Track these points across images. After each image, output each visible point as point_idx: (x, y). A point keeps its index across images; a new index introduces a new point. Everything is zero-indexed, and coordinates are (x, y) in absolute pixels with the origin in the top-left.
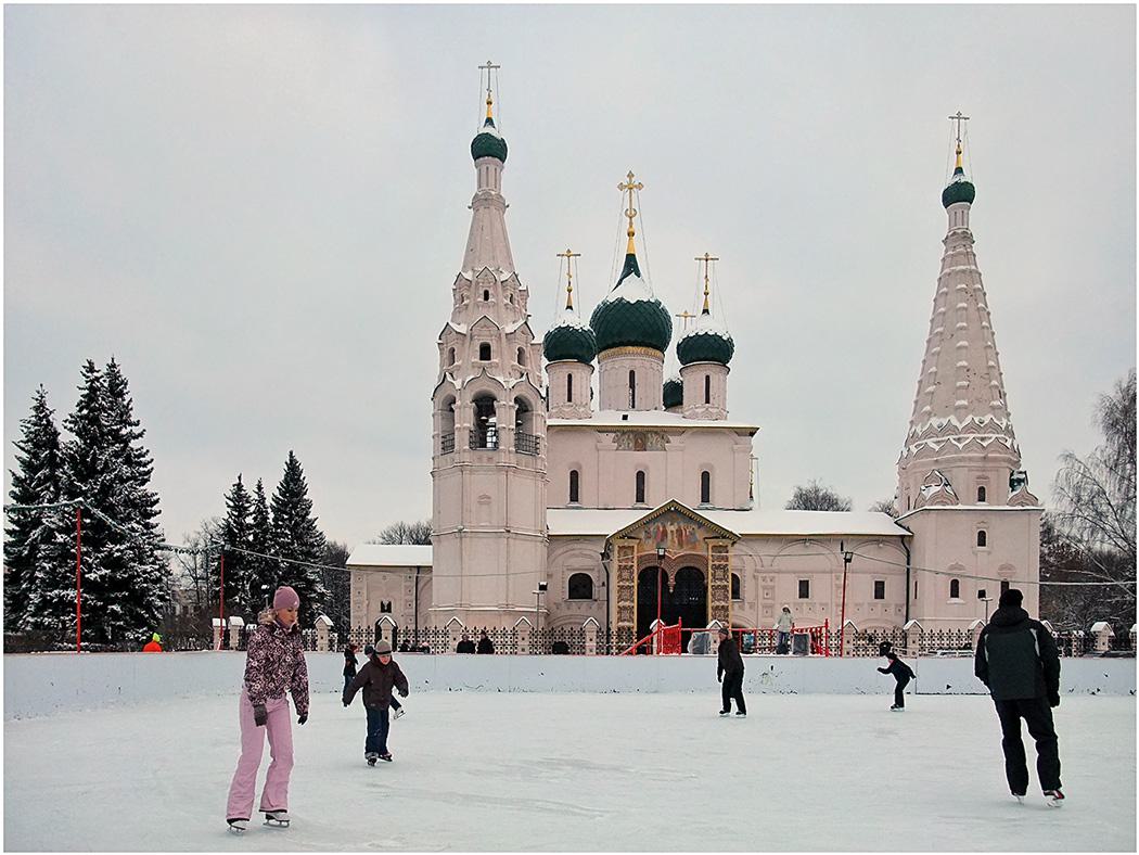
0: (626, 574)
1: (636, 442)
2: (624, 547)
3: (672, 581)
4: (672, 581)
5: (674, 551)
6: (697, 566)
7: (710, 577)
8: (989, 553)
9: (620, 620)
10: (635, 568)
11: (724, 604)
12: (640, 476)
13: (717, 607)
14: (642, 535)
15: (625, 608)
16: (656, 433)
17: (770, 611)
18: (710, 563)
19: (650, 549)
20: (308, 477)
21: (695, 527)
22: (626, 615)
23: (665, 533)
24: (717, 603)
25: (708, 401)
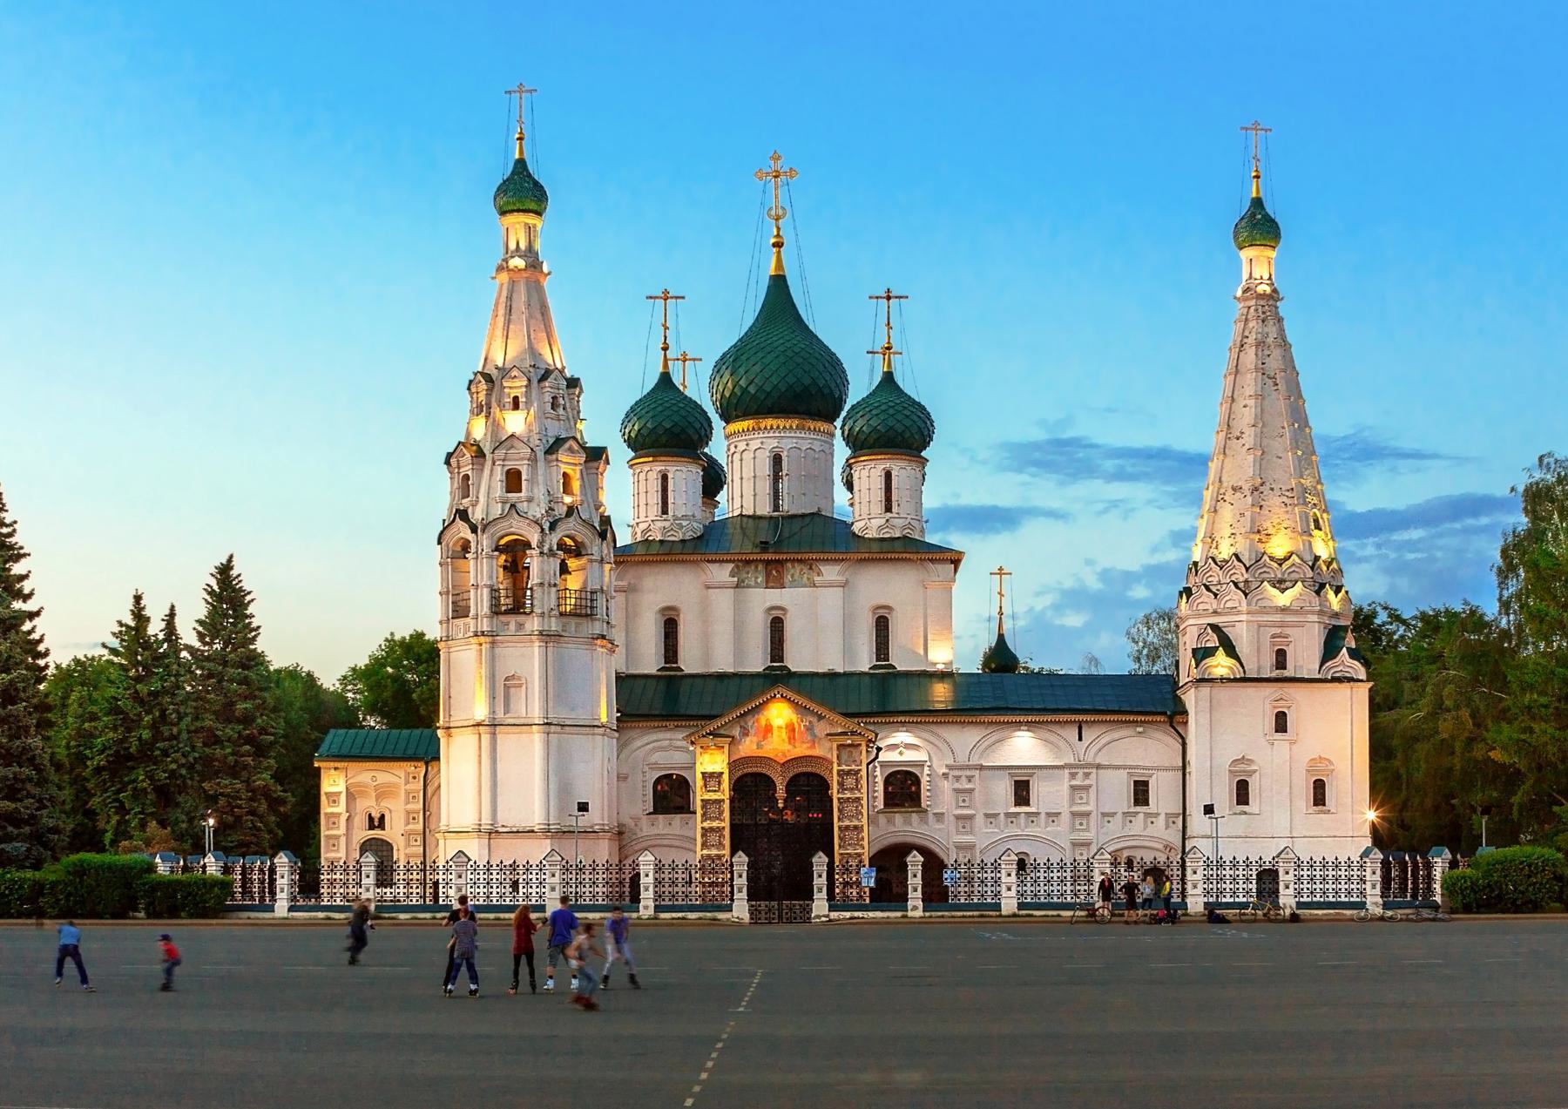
1: (768, 575)
3: (781, 792)
4: (781, 792)
7: (835, 791)
8: (1293, 742)
9: (704, 845)
10: (726, 777)
11: (856, 823)
12: (777, 627)
13: (847, 828)
14: (736, 732)
15: (712, 829)
16: (800, 561)
17: (968, 826)
18: (836, 768)
21: (814, 720)
22: (713, 838)
24: (847, 823)
25: (888, 509)
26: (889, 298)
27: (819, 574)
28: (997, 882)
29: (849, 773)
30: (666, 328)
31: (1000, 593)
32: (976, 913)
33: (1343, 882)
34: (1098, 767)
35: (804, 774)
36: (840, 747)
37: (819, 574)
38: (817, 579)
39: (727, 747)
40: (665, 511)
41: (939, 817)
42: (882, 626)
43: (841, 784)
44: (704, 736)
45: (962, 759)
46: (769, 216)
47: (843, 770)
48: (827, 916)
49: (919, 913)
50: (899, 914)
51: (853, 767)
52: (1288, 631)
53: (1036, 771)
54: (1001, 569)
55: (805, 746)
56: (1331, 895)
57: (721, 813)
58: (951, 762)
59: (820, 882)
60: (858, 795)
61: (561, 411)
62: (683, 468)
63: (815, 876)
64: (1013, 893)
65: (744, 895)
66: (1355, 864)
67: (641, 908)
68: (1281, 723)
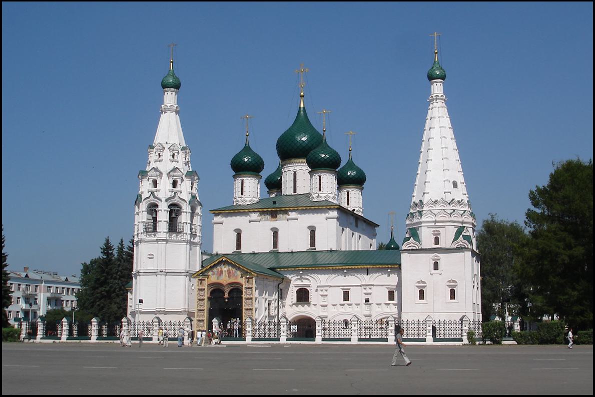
0: (202, 293)
3: (226, 295)
4: (226, 295)
5: (225, 279)
13: (247, 309)
18: (244, 286)
19: (213, 278)
23: (221, 272)
24: (247, 307)
25: (320, 190)
27: (289, 215)
29: (248, 288)
33: (416, 330)
34: (373, 285)
37: (289, 215)
38: (288, 217)
39: (206, 279)
40: (242, 194)
41: (315, 305)
45: (323, 284)
52: (438, 229)
53: (351, 287)
55: (234, 278)
56: (410, 336)
57: (204, 304)
58: (319, 285)
61: (175, 157)
62: (249, 179)
66: (421, 322)
68: (436, 266)
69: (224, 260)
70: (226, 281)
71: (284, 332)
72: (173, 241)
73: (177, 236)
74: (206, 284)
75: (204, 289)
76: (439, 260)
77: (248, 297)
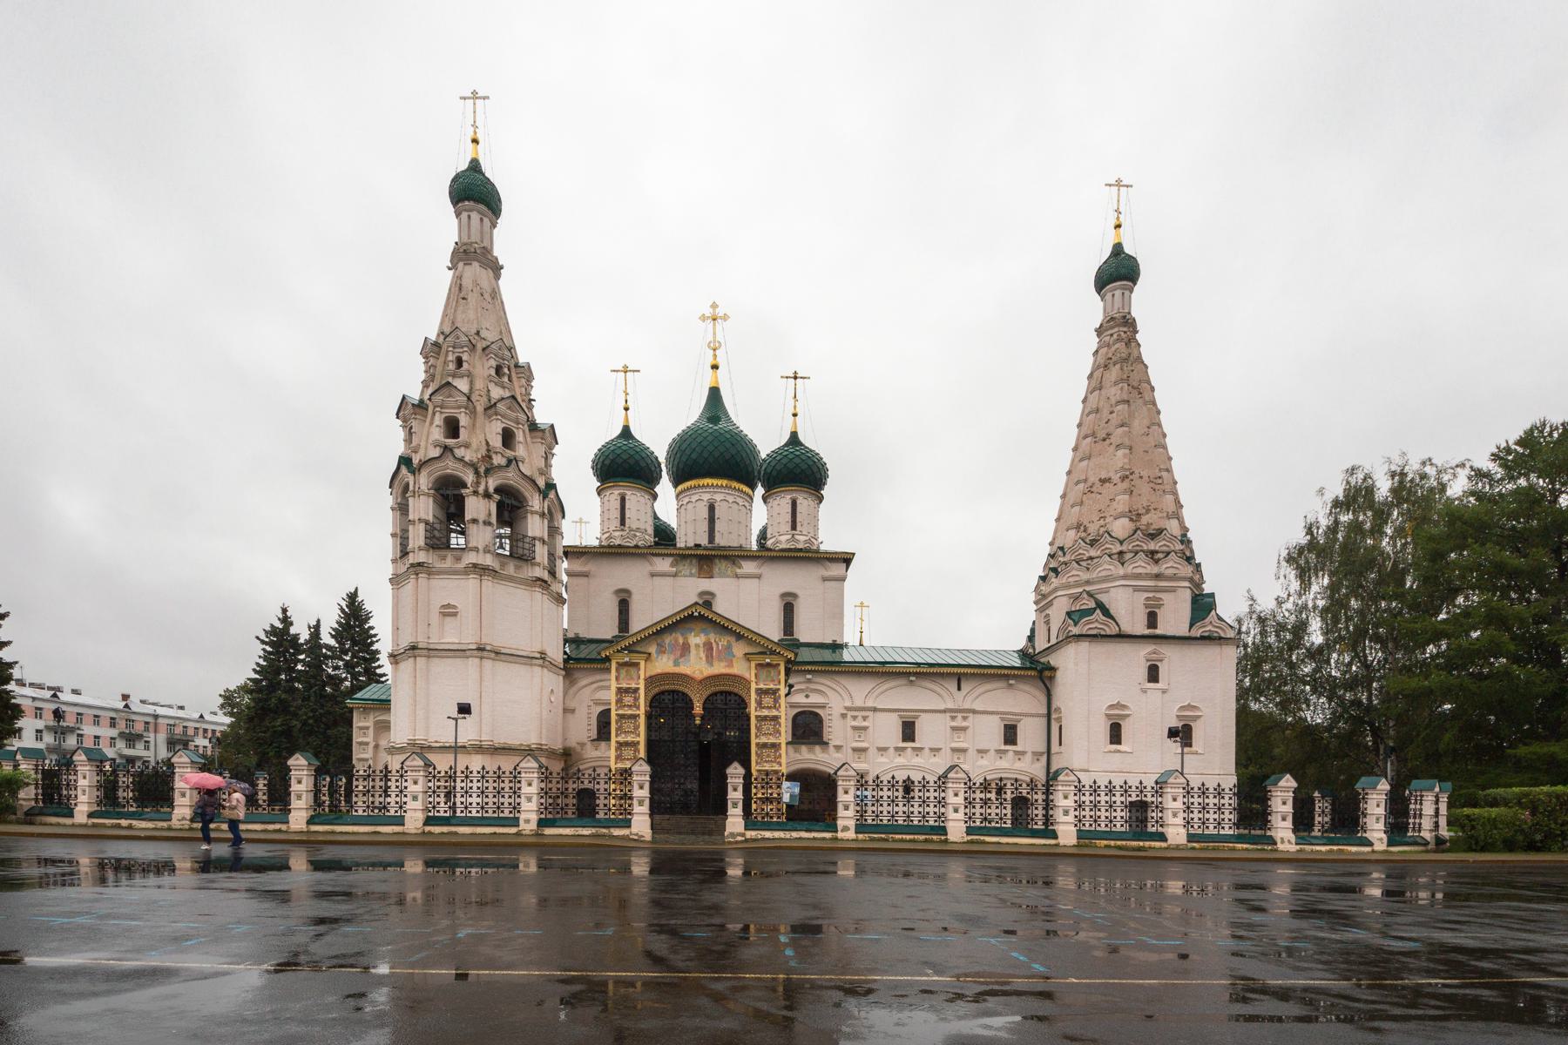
0: (628, 700)
2: (626, 664)
3: (698, 709)
4: (698, 709)
5: (697, 666)
6: (736, 690)
7: (753, 705)
10: (642, 692)
11: (772, 740)
13: (765, 745)
14: (653, 649)
18: (753, 686)
19: (663, 664)
20: (322, 623)
21: (732, 639)
23: (686, 649)
26: (795, 378)
28: (941, 802)
30: (627, 394)
31: (861, 619)
32: (922, 837)
35: (721, 693)
36: (759, 666)
42: (789, 610)
43: (759, 703)
44: (618, 651)
46: (709, 347)
47: (761, 689)
48: (743, 835)
49: (851, 835)
50: (828, 835)
51: (772, 686)
54: (862, 603)
55: (723, 664)
57: (636, 728)
59: (735, 795)
60: (774, 713)
63: (730, 788)
64: (960, 815)
65: (645, 808)
67: (521, 822)
68: (1153, 674)
69: (696, 614)
70: (701, 672)
71: (956, 811)
72: (510, 579)
73: (517, 568)
74: (642, 677)
75: (637, 690)
76: (1161, 661)
77: (765, 713)
